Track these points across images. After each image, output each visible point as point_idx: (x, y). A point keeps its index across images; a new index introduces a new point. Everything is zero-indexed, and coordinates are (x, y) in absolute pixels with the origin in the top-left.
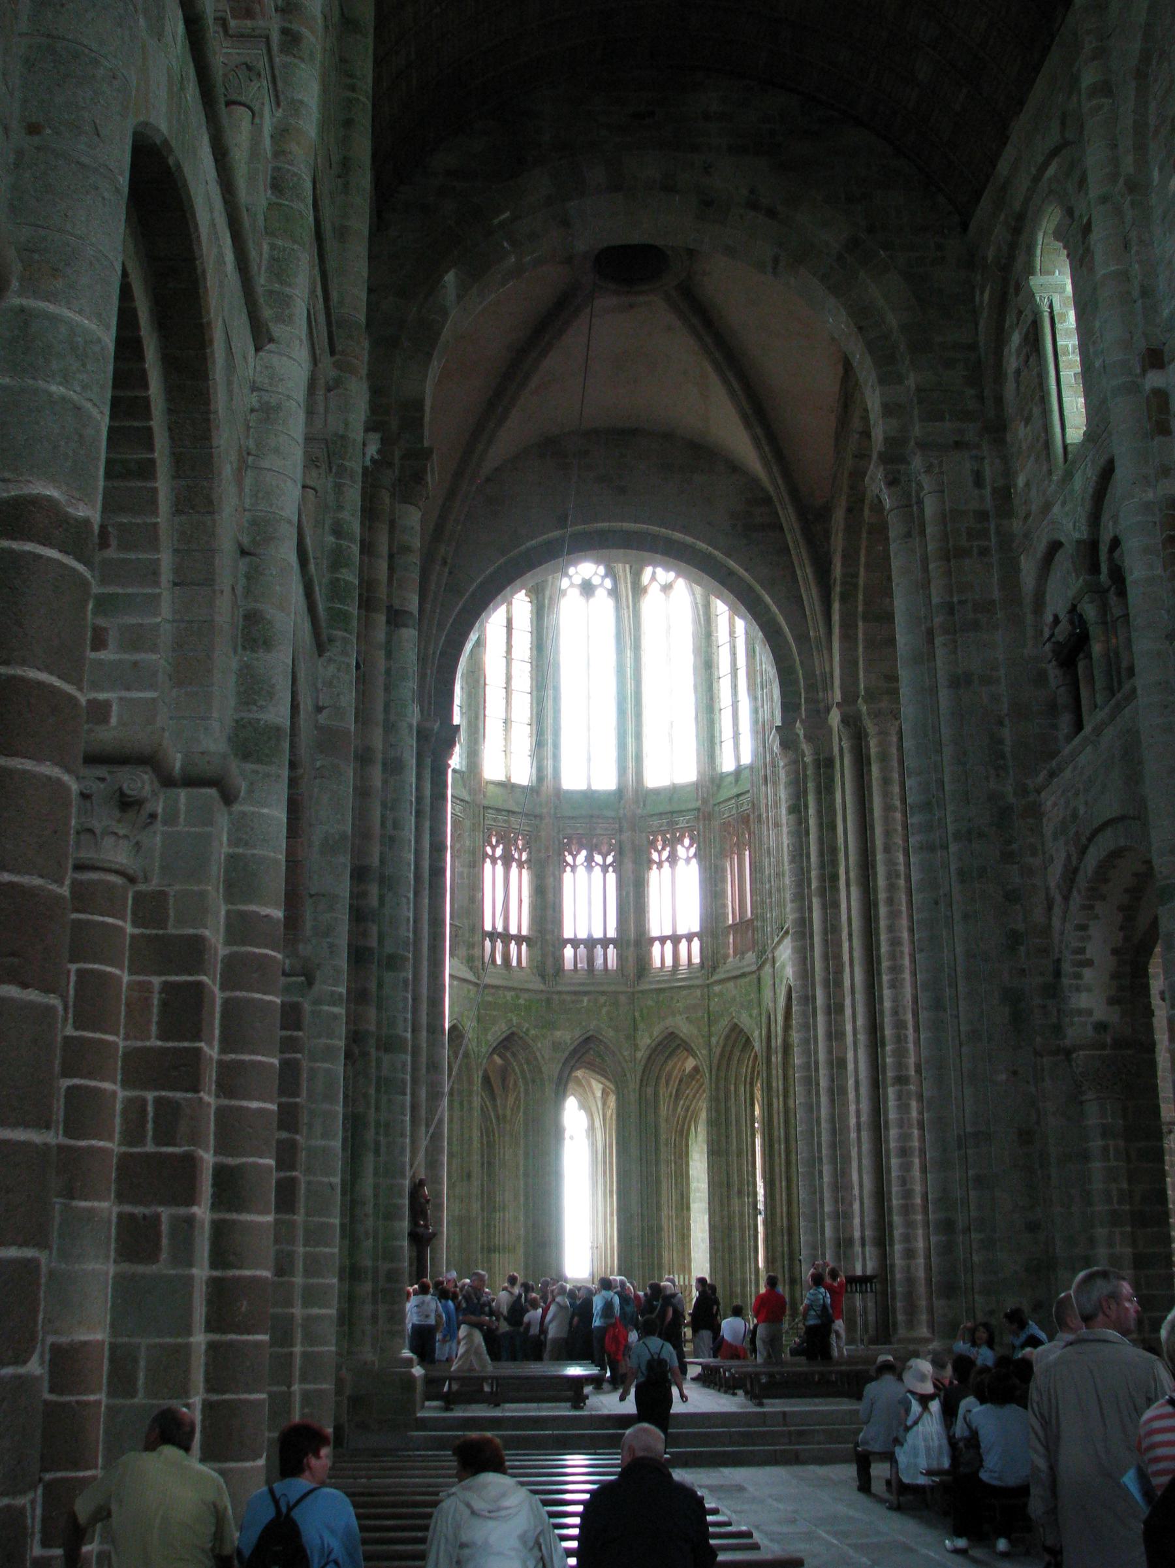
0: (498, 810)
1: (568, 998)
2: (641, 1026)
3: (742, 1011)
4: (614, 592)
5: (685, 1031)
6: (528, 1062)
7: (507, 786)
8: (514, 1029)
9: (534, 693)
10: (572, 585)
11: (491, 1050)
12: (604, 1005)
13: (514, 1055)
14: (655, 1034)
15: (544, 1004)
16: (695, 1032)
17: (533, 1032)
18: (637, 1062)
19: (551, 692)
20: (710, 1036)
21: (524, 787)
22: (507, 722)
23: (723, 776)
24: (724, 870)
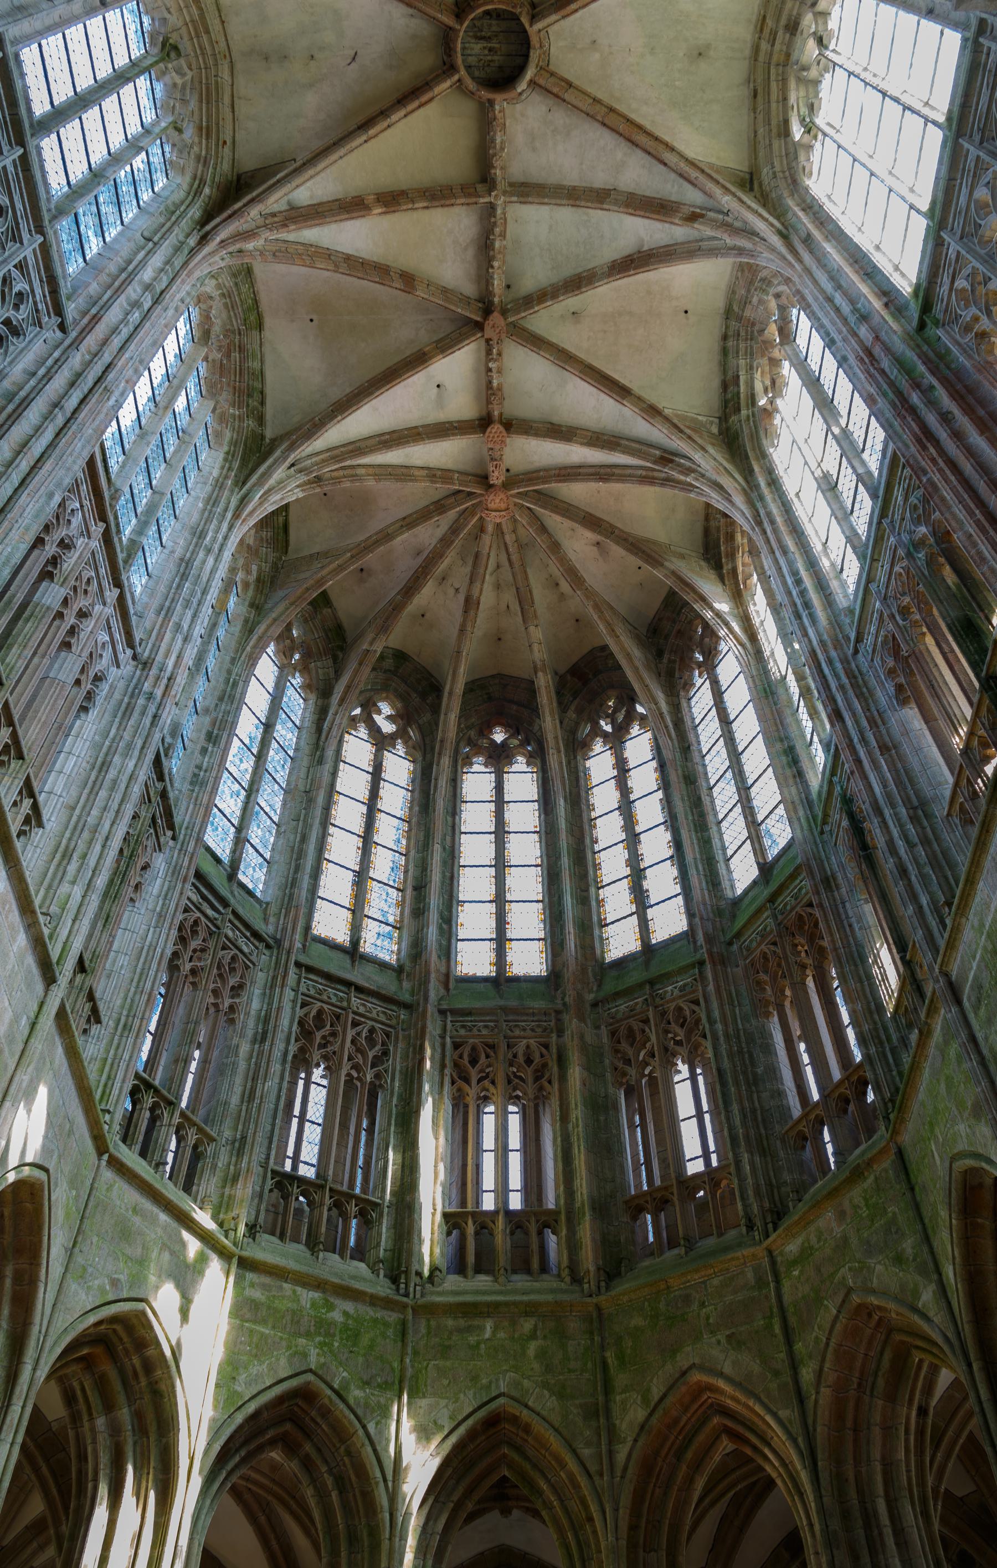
0: (329, 977)
1: (450, 1323)
2: (621, 1379)
3: (871, 1262)
4: (538, 757)
5: (727, 1369)
6: (341, 1483)
7: (353, 951)
8: (310, 1377)
9: (412, 853)
10: (478, 750)
11: (239, 1418)
12: (533, 1336)
13: (307, 1464)
14: (656, 1393)
15: (390, 1332)
16: (756, 1368)
17: (356, 1394)
18: (618, 1473)
19: (437, 847)
20: (794, 1366)
21: (383, 965)
22: (361, 878)
23: (737, 902)
24: (766, 1036)
